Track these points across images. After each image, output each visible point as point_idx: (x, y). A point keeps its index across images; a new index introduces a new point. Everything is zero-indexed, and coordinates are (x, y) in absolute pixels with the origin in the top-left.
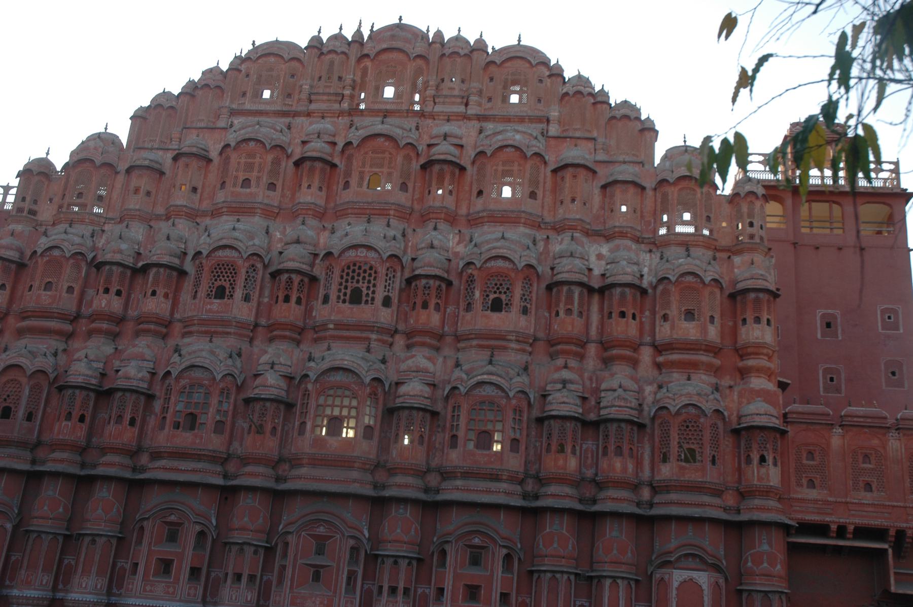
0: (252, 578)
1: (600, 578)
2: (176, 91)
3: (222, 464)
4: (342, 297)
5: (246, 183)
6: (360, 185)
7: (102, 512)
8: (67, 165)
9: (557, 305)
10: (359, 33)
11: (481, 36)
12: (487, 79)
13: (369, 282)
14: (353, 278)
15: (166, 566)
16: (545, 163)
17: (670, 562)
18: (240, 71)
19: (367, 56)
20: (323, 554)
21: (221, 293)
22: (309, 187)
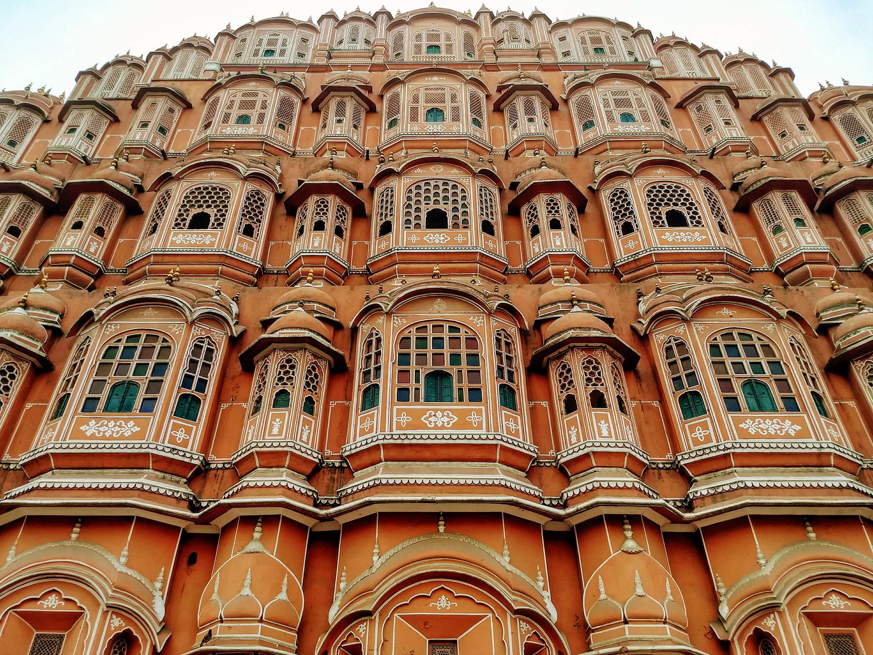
3: (189, 482)
4: (414, 222)
5: (244, 120)
6: (414, 117)
12: (556, 42)
14: (427, 198)
16: (666, 96)
18: (235, 38)
21: (200, 222)
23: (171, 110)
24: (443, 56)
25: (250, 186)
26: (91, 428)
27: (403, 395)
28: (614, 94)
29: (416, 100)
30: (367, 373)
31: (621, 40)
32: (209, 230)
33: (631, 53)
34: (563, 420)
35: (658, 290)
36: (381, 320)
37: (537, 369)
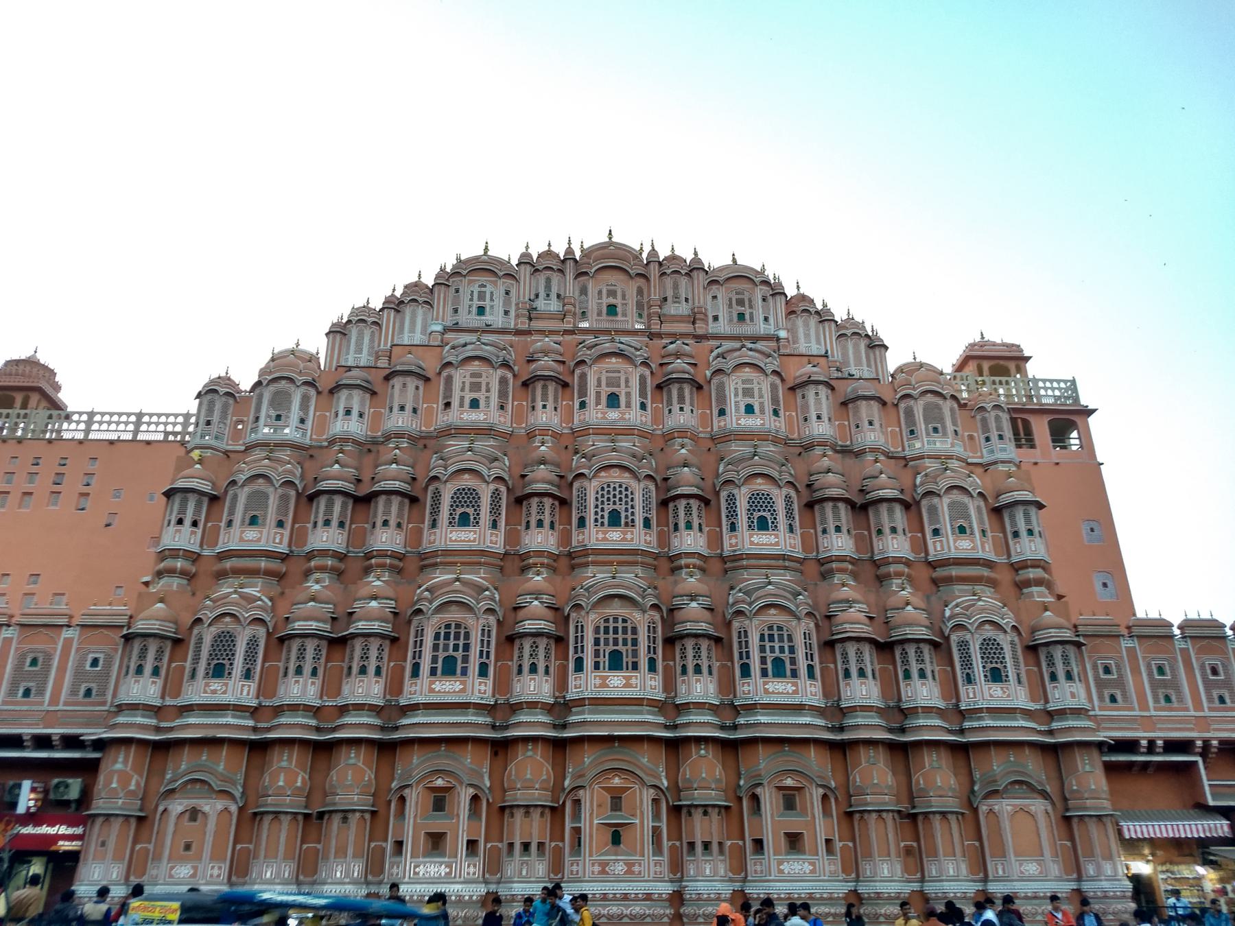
0: (541, 845)
1: (926, 814)
2: (377, 304)
5: (475, 404)
7: (352, 779)
8: (258, 384)
9: (824, 521)
10: (569, 251)
11: (696, 254)
12: (709, 298)
13: (627, 503)
14: (609, 499)
15: (436, 842)
17: (996, 791)
19: (586, 273)
20: (620, 810)
21: (464, 520)
22: (544, 407)
23: (417, 388)
24: (621, 322)
25: (492, 487)
26: (437, 686)
27: (597, 666)
28: (744, 382)
29: (599, 385)
30: (576, 648)
31: (760, 301)
32: (471, 528)
33: (766, 319)
34: (679, 679)
35: (740, 590)
36: (583, 613)
37: (670, 641)
